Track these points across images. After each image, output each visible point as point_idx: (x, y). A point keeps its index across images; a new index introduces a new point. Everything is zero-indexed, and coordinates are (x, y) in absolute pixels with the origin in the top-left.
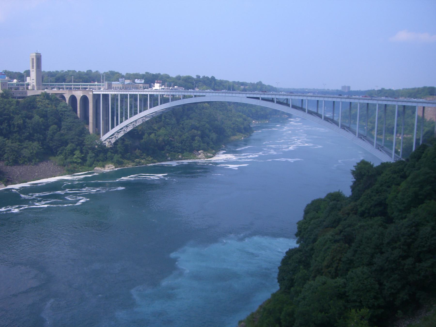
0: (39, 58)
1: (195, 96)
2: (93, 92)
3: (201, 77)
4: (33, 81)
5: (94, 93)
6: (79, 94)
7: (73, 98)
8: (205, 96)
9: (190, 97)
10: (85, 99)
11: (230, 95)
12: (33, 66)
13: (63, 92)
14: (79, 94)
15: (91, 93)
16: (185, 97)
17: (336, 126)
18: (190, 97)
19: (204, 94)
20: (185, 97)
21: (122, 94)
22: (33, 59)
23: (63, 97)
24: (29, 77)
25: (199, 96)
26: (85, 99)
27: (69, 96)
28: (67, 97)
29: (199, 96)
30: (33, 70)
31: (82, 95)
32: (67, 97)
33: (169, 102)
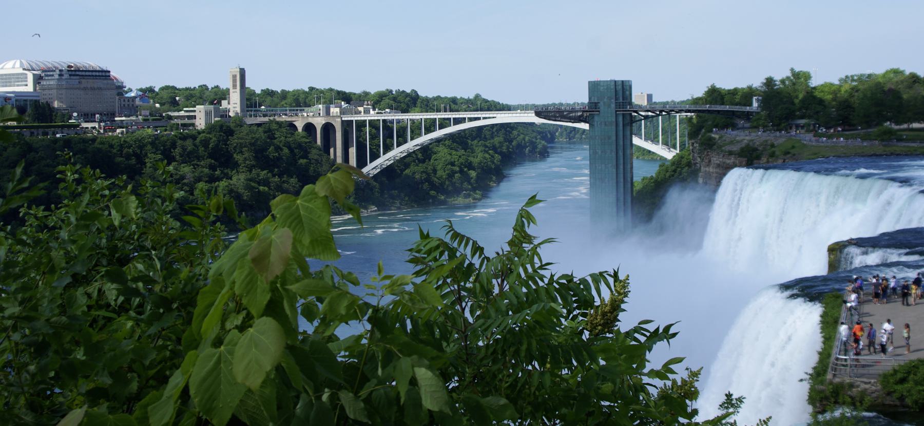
0: (242, 72)
1: (484, 118)
2: (341, 118)
3: (401, 90)
4: (235, 106)
5: (343, 119)
6: (319, 122)
7: (309, 128)
8: (493, 117)
9: (479, 119)
10: (328, 129)
11: (526, 115)
12: (234, 86)
14: (319, 122)
15: (339, 120)
16: (471, 120)
18: (479, 119)
19: (494, 115)
20: (471, 120)
21: (372, 120)
22: (234, 77)
23: (292, 126)
25: (489, 118)
28: (300, 125)
29: (489, 118)
30: (234, 90)
31: (324, 122)
32: (300, 125)
33: (450, 126)
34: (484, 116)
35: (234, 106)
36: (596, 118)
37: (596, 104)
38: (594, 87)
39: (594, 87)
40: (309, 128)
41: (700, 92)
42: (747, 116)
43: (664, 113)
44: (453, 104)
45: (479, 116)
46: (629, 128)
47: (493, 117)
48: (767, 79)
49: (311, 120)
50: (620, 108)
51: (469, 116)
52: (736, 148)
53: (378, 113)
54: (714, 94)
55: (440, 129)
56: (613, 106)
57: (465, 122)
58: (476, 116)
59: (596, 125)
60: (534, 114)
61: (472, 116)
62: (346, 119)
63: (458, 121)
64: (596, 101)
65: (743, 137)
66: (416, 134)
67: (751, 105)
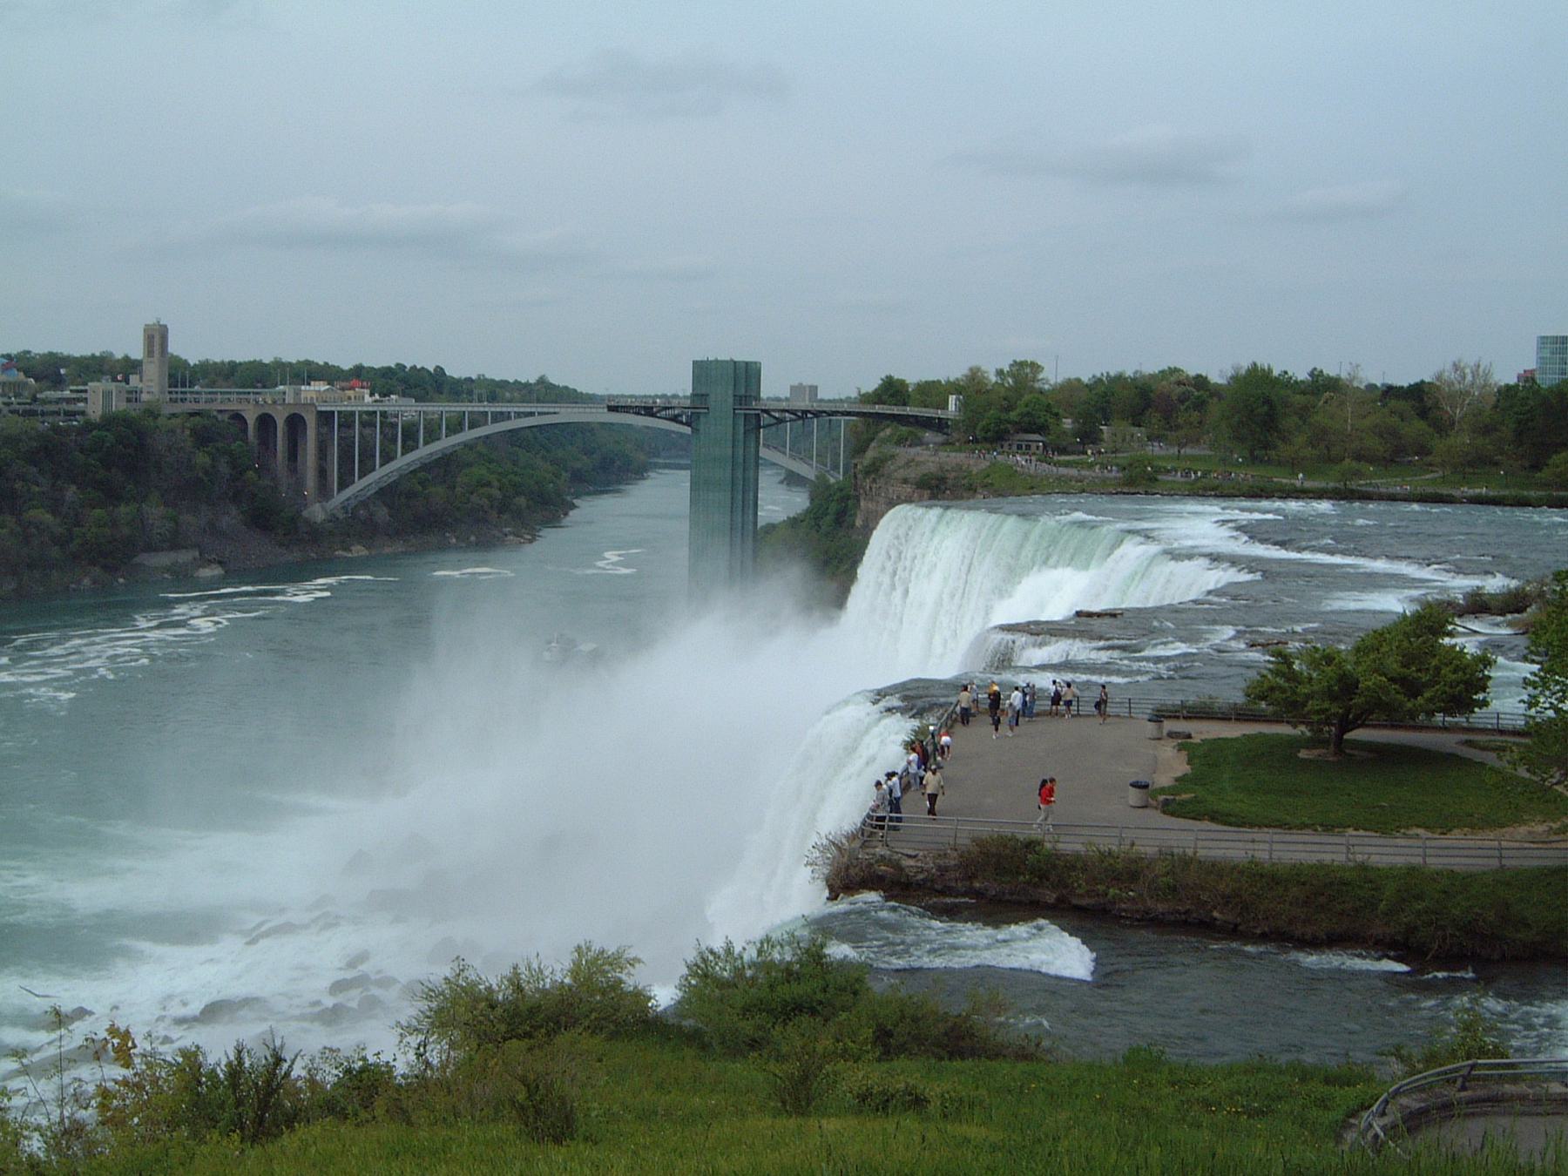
4: (150, 384)
5: (319, 409)
7: (266, 421)
8: (555, 413)
9: (532, 414)
10: (295, 422)
13: (240, 408)
16: (519, 415)
17: (782, 455)
18: (532, 414)
19: (557, 410)
20: (519, 415)
24: (138, 377)
25: (548, 413)
26: (295, 422)
27: (256, 415)
28: (251, 418)
29: (548, 413)
30: (150, 359)
32: (251, 418)
33: (486, 423)
34: (540, 410)
35: (150, 384)
36: (702, 419)
37: (704, 396)
38: (702, 370)
39: (702, 370)
40: (266, 421)
41: (871, 385)
42: (939, 425)
43: (809, 415)
44: (495, 390)
45: (533, 410)
46: (753, 436)
47: (555, 413)
48: (971, 369)
49: (267, 410)
50: (741, 404)
51: (516, 409)
52: (913, 473)
53: (376, 401)
54: (892, 390)
55: (470, 428)
56: (731, 400)
57: (509, 418)
58: (528, 410)
59: (701, 431)
60: (606, 410)
61: (522, 410)
62: (323, 409)
63: (499, 417)
64: (703, 392)
65: (929, 456)
66: (432, 436)
67: (944, 406)
